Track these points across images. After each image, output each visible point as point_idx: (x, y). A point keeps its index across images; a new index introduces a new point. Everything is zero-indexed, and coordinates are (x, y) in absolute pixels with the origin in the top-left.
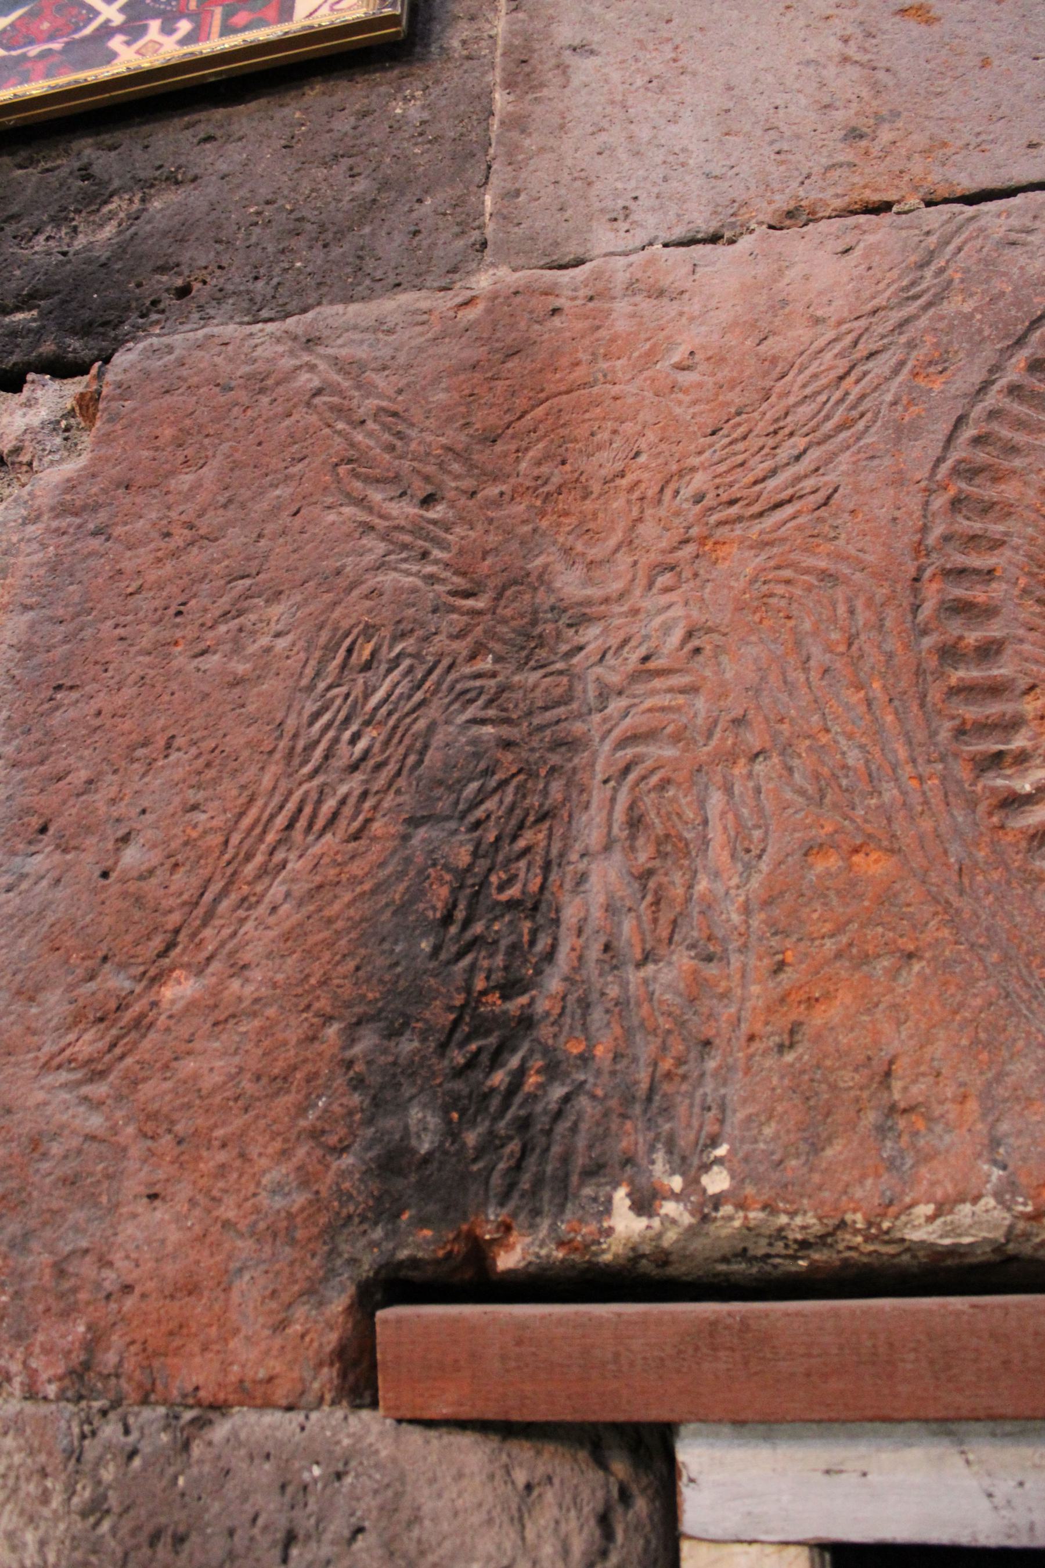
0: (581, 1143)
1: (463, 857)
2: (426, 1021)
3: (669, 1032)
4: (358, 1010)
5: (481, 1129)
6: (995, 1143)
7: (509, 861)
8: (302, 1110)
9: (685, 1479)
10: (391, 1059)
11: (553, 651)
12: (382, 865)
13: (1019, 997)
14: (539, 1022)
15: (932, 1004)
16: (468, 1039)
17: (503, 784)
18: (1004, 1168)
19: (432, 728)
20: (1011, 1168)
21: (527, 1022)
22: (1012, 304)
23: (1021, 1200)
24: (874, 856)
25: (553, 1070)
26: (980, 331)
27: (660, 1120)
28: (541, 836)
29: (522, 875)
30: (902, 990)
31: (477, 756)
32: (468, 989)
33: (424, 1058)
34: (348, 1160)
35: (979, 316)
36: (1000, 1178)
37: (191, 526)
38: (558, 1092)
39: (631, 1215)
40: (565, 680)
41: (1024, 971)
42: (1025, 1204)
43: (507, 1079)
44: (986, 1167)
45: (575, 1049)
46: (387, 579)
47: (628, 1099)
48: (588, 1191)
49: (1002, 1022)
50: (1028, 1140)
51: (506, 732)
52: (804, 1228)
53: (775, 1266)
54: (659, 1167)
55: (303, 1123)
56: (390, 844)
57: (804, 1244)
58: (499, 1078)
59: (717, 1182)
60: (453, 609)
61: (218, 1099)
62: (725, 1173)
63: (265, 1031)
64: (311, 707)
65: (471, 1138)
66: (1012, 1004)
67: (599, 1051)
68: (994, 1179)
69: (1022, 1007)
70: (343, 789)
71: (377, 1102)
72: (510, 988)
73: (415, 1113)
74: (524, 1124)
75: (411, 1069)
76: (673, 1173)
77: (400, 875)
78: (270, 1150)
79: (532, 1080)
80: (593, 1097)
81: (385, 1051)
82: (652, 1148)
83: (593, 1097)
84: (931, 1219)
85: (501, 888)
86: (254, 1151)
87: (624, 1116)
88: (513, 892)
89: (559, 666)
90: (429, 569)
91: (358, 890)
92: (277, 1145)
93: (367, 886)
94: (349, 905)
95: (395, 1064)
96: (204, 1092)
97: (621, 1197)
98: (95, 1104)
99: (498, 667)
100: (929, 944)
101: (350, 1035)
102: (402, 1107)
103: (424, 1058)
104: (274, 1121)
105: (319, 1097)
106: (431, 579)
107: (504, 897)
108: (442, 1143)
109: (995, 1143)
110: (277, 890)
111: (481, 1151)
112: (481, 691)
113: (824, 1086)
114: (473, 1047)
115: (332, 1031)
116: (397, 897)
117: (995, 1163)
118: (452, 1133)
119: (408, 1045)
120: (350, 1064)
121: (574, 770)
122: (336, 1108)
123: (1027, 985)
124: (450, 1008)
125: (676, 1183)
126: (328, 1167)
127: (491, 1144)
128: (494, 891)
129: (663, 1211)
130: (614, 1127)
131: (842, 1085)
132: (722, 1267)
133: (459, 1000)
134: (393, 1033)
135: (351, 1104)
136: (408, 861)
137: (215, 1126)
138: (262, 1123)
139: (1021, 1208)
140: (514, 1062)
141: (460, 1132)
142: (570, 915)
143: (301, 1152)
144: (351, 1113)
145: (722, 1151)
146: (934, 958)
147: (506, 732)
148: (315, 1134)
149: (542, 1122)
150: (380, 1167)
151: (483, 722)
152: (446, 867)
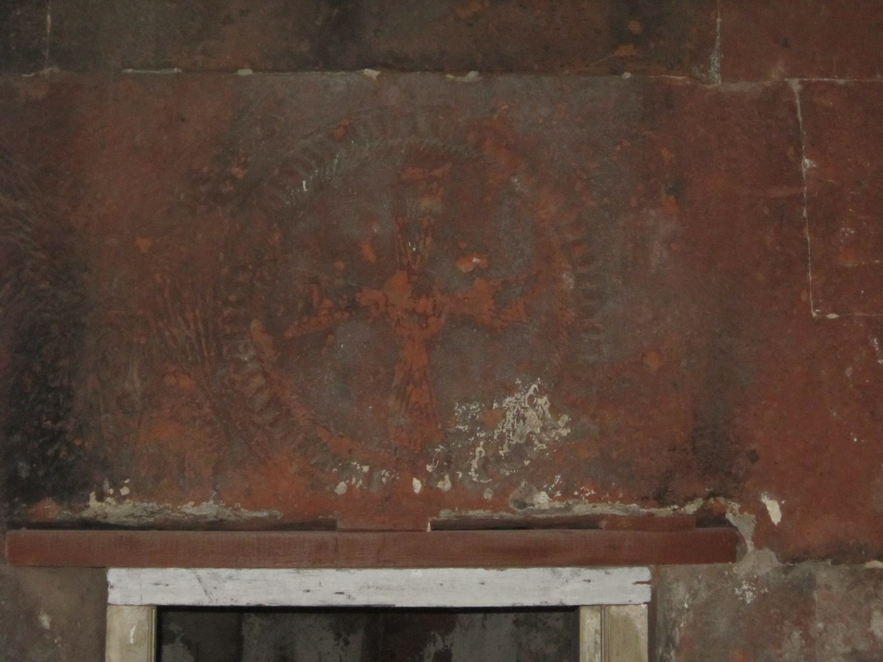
1: (38, 368)
9: (109, 586)
21: (61, 432)
23: (221, 502)
38: (72, 458)
39: (96, 501)
42: (223, 503)
48: (81, 493)
52: (152, 507)
53: (143, 520)
54: (106, 485)
57: (153, 513)
58: (50, 452)
59: (125, 491)
65: (40, 473)
72: (56, 419)
79: (63, 453)
84: (193, 506)
88: (56, 384)
90: (22, 236)
97: (93, 495)
107: (53, 385)
114: (41, 441)
119: (17, 438)
125: (111, 491)
128: (50, 383)
129: (106, 501)
132: (125, 519)
133: (36, 423)
139: (221, 504)
140: (56, 447)
145: (127, 481)
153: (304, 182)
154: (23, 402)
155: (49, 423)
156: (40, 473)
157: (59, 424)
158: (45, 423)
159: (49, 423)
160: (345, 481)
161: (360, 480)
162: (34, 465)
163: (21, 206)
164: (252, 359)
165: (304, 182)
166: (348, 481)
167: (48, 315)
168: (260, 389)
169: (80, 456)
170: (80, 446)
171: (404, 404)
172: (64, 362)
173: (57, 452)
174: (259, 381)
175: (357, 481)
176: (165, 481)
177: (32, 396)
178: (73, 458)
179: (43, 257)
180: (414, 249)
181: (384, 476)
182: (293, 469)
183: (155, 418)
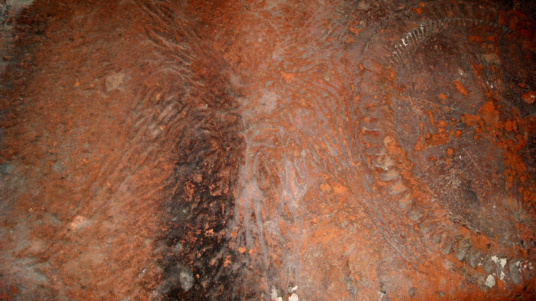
0: (245, 285)
2: (186, 240)
3: (275, 246)
4: (159, 234)
5: (208, 281)
6: (382, 285)
7: (215, 182)
8: (136, 274)
10: (172, 254)
11: (230, 105)
12: (167, 180)
13: (387, 237)
14: (228, 241)
15: (361, 238)
16: (202, 247)
17: (213, 152)
18: (385, 293)
19: (185, 128)
20: (387, 293)
22: (379, 10)
24: (341, 188)
25: (234, 259)
26: (370, 17)
27: (274, 278)
28: (227, 172)
29: (221, 187)
30: (351, 233)
31: (204, 141)
32: (202, 228)
33: (185, 254)
34: (155, 294)
35: (369, 12)
36: (383, 296)
37: (82, 37)
38: (236, 267)
40: (235, 117)
41: (388, 228)
43: (218, 262)
44: (379, 293)
45: (242, 250)
46: (165, 70)
47: (261, 270)
49: (382, 245)
50: (392, 284)
51: (214, 133)
55: (137, 280)
56: (171, 172)
58: (213, 261)
60: (191, 84)
61: (99, 270)
62: (296, 296)
63: (121, 243)
64: (136, 115)
65: (204, 284)
66: (385, 239)
67: (251, 252)
68: (382, 296)
69: (388, 240)
70: (150, 149)
71: (167, 270)
72: (217, 229)
73: (183, 275)
74: (223, 279)
75: (183, 258)
76: (278, 297)
77: (173, 185)
78: (123, 291)
79: (227, 262)
80: (250, 269)
81: (170, 251)
82: (271, 288)
83: (250, 269)
85: (213, 190)
86: (116, 291)
87: (261, 276)
88: (218, 193)
89: (232, 111)
91: (157, 189)
92: (126, 288)
93: (161, 187)
94: (154, 194)
95: (174, 256)
96: (93, 267)
98: (43, 272)
99: (210, 109)
100: (360, 218)
101: (155, 244)
102: (178, 272)
103: (185, 254)
104: (125, 279)
105: (143, 269)
106: (183, 72)
108: (194, 286)
109: (382, 285)
110: (123, 187)
111: (208, 289)
112: (203, 116)
113: (328, 266)
114: (204, 250)
115: (148, 242)
116: (173, 192)
117: (382, 291)
118: (197, 282)
120: (154, 255)
121: (239, 150)
122: (151, 273)
123: (389, 233)
124: (195, 235)
126: (148, 297)
127: (211, 285)
128: (211, 192)
130: (257, 280)
131: (333, 265)
133: (199, 232)
134: (171, 243)
135: (157, 272)
136: (177, 179)
137: (99, 281)
138: (119, 279)
140: (219, 256)
141: (200, 282)
142: (239, 202)
143: (136, 291)
144: (157, 275)
145: (295, 288)
146: (361, 223)
147: (214, 133)
148: (143, 284)
149: (232, 278)
150: (169, 296)
151: (205, 129)
152: (192, 182)
153: (403, 40)
154: (184, 211)
155: (211, 231)
156: (204, 284)
157: (222, 233)
158: (207, 232)
159: (211, 231)
160: (491, 273)
161: (502, 272)
162: (198, 276)
163: (181, 47)
164: (391, 168)
165: (403, 40)
166: (494, 274)
167: (208, 132)
168: (403, 194)
169: (245, 264)
170: (244, 253)
171: (520, 203)
172: (225, 173)
173: (221, 261)
174: (398, 188)
175: (500, 273)
176: (333, 285)
177: (194, 206)
178: (238, 266)
179: (202, 85)
180: (492, 87)
181: (519, 267)
182: (447, 265)
183: (315, 223)
